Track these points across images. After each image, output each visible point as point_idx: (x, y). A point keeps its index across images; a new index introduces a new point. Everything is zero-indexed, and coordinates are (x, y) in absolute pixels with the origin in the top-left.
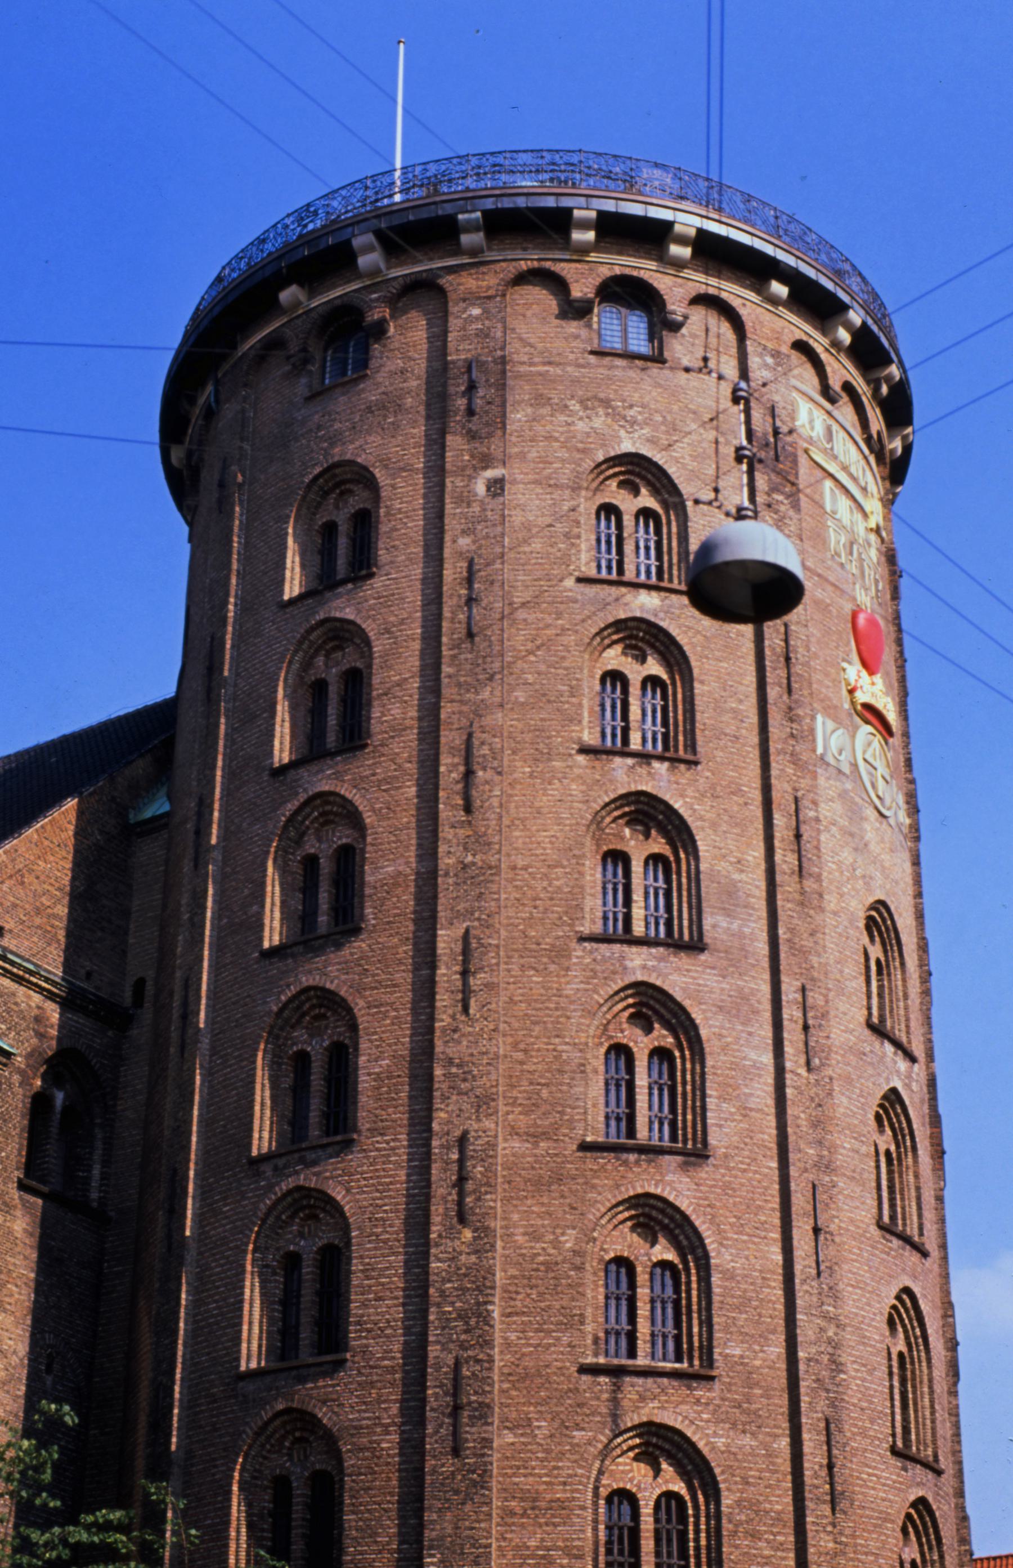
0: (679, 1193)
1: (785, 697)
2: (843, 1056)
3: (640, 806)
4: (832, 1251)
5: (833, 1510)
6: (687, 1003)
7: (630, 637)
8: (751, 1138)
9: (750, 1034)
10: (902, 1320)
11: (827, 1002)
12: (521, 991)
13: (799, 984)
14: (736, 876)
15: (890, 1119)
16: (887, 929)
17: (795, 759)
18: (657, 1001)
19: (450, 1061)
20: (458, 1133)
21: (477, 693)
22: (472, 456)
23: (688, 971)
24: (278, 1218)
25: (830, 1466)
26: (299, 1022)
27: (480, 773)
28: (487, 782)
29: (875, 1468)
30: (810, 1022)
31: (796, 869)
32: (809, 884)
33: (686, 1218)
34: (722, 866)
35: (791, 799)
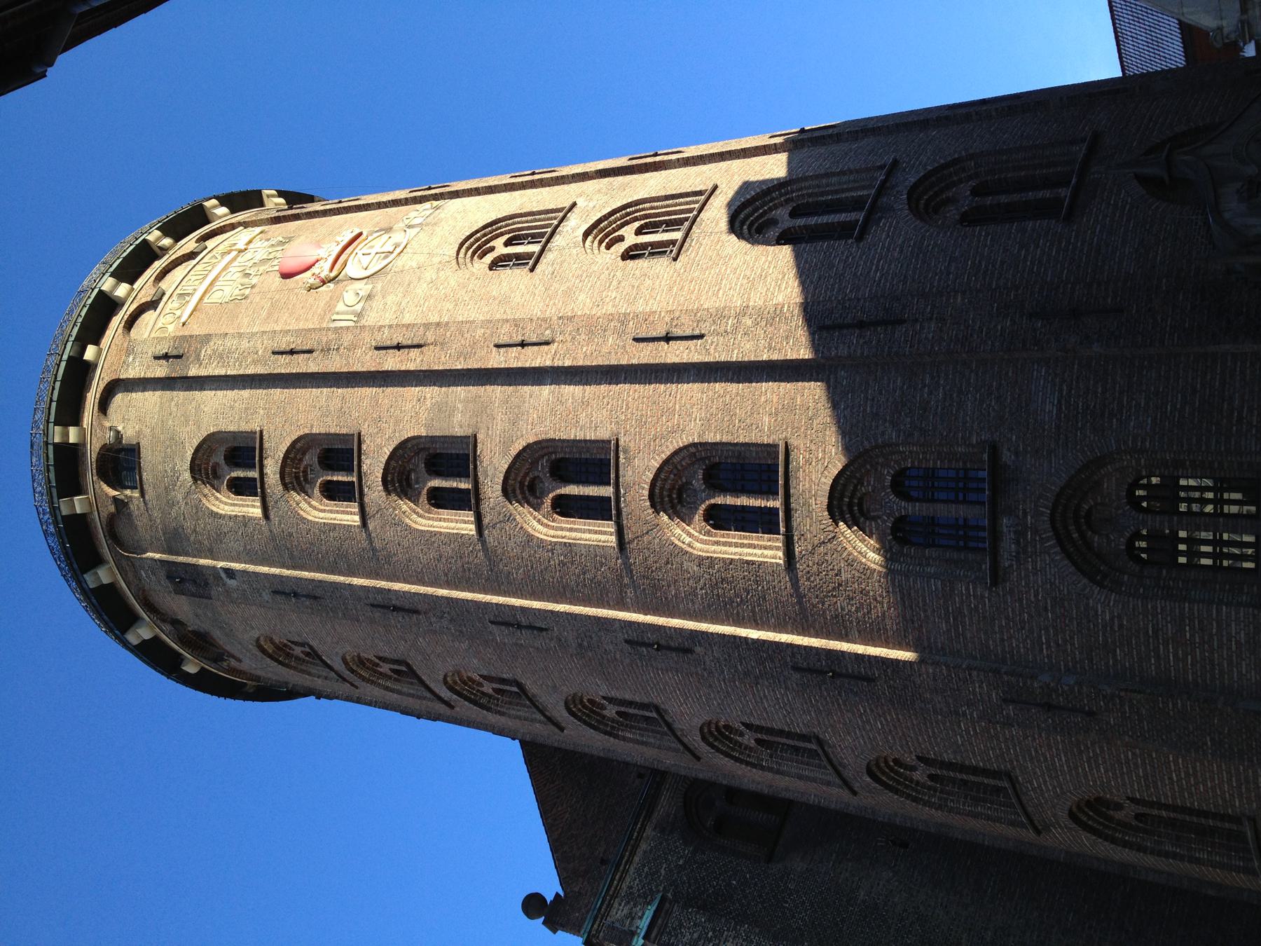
0: (648, 468)
3: (396, 479)
4: (685, 319)
5: (901, 322)
6: (514, 452)
7: (297, 478)
8: (604, 398)
9: (531, 396)
10: (761, 216)
11: (507, 321)
12: (525, 587)
14: (428, 403)
15: (615, 231)
16: (485, 235)
17: (352, 347)
18: (517, 475)
19: (580, 645)
20: (627, 646)
21: (347, 598)
22: (218, 585)
24: (733, 750)
25: (861, 325)
26: (599, 714)
27: (393, 602)
28: (397, 599)
29: (872, 263)
30: (520, 339)
32: (430, 337)
33: (666, 462)
34: (423, 417)
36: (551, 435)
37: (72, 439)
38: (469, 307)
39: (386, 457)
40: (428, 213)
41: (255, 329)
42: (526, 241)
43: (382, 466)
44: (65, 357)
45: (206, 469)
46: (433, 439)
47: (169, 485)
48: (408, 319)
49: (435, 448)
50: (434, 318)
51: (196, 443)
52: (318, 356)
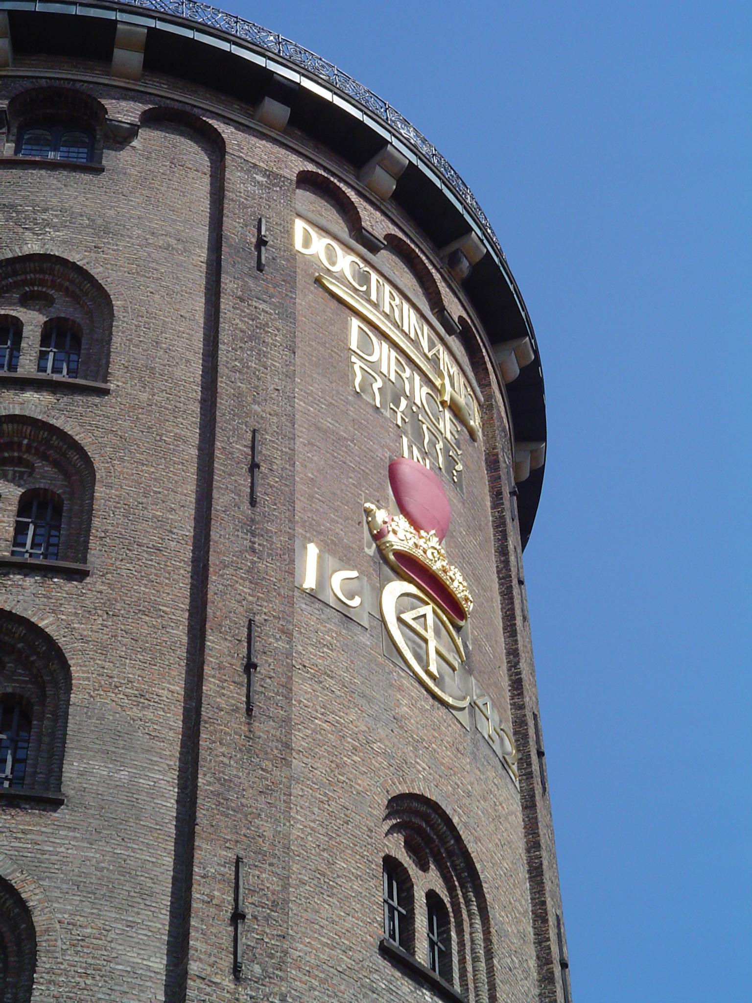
1: (246, 506)
2: (322, 981)
11: (286, 887)
13: (231, 855)
17: (255, 579)
23: (23, 832)
30: (249, 911)
31: (244, 706)
32: (264, 728)
35: (244, 622)
36: (44, 963)
37: (120, 55)
38: (316, 810)
39: (34, 620)
40: (496, 747)
41: (299, 404)
42: (435, 938)
43: (18, 610)
44: (273, 67)
45: (42, 283)
46: (61, 717)
47: (17, 212)
48: (303, 688)
49: (41, 719)
50: (299, 740)
51: (96, 271)
52: (243, 513)
